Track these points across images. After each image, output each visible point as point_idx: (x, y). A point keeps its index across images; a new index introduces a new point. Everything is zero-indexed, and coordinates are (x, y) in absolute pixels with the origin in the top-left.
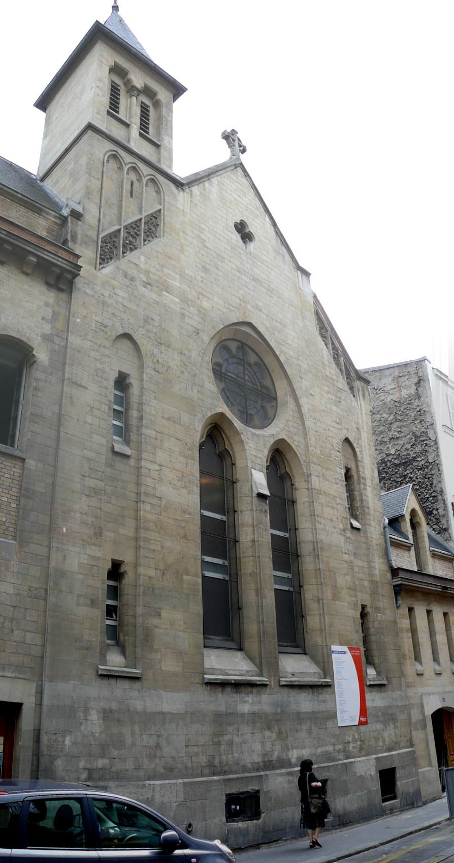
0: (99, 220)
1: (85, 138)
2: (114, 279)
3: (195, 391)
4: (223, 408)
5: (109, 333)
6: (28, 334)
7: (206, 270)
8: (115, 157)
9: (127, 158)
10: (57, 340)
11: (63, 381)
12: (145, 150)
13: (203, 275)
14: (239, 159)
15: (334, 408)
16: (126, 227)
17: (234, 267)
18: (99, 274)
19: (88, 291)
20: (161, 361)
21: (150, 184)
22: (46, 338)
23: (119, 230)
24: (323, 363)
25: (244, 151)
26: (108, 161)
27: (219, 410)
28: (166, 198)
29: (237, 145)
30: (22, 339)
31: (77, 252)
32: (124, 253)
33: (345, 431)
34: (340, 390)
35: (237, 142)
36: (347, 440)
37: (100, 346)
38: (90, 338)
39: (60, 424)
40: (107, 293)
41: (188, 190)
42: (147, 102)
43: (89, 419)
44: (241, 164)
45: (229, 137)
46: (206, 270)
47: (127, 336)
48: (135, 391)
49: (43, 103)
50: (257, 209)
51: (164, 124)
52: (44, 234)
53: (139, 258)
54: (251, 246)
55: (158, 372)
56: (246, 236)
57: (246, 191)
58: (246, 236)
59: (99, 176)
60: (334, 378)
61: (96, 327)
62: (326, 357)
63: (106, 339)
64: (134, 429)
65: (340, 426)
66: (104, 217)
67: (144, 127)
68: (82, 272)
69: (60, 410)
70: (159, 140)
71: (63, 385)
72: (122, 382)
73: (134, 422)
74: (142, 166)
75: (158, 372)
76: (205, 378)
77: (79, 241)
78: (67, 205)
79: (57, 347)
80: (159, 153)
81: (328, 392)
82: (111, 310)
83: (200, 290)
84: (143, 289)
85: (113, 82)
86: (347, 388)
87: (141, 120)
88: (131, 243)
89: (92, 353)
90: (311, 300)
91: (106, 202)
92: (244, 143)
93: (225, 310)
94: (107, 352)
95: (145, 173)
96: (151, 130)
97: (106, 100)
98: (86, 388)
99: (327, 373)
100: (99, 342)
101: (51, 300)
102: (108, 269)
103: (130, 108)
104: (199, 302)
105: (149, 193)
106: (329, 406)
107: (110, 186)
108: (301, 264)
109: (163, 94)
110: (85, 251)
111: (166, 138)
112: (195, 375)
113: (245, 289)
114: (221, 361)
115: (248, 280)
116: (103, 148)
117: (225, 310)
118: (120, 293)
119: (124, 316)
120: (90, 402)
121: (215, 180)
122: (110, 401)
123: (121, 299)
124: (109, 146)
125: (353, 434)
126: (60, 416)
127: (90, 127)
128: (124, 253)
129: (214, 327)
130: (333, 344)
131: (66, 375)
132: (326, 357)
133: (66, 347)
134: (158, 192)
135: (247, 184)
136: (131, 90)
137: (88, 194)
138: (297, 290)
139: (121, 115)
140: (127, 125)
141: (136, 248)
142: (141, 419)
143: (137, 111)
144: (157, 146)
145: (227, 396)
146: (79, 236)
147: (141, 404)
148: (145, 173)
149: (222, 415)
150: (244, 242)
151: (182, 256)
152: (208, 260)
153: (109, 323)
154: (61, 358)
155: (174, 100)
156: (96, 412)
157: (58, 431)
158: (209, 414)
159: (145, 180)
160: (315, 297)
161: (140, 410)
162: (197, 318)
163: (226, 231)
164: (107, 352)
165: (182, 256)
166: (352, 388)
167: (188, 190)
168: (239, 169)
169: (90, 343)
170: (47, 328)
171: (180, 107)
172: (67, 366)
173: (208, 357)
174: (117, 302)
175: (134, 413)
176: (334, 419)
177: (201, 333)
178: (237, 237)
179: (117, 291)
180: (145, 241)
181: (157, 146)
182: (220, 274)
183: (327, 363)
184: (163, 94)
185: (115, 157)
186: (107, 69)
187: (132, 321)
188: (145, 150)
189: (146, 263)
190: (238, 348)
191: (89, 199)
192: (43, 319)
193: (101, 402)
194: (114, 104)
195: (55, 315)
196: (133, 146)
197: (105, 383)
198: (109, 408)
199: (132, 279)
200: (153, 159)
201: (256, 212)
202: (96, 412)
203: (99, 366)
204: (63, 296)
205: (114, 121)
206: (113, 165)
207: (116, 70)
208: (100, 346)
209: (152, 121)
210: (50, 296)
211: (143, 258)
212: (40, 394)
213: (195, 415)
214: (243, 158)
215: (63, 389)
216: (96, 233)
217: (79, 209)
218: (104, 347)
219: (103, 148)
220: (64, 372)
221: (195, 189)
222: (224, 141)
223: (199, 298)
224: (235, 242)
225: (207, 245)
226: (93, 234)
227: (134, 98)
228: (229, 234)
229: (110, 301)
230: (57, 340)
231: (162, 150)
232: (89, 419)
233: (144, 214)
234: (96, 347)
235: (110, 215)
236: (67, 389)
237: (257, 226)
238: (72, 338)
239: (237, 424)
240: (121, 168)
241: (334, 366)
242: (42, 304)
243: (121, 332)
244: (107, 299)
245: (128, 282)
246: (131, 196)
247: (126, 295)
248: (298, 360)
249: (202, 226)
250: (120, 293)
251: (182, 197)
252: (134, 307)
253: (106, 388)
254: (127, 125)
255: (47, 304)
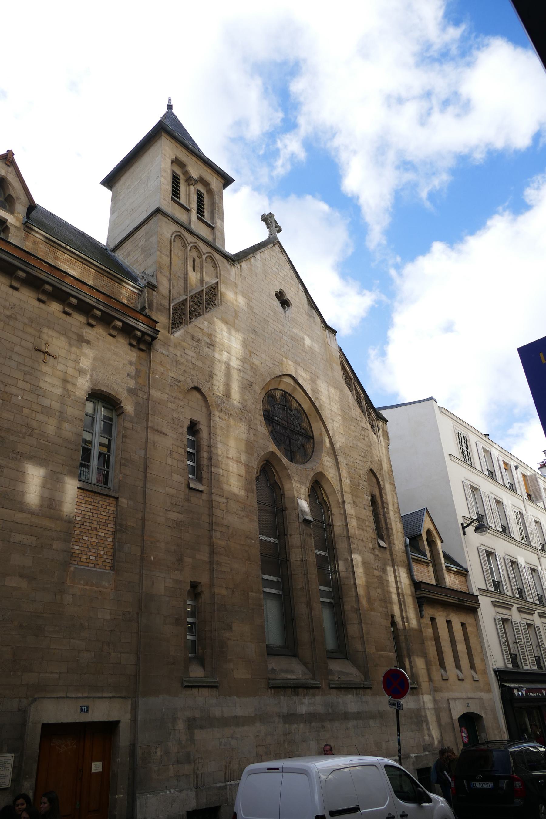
0: (170, 291)
1: (154, 220)
2: (184, 341)
3: (252, 434)
4: (272, 447)
5: (182, 387)
6: (116, 389)
7: (255, 332)
8: (180, 236)
9: (190, 239)
10: (140, 394)
11: (147, 428)
12: (203, 231)
13: (253, 336)
14: (276, 238)
15: (360, 444)
16: (191, 297)
17: (277, 329)
18: (172, 337)
19: (164, 352)
20: (224, 409)
21: (208, 260)
22: (132, 392)
23: (186, 299)
24: (349, 407)
25: (279, 231)
26: (174, 240)
27: (271, 450)
28: (222, 273)
29: (274, 226)
30: (112, 392)
31: (154, 318)
32: (190, 319)
33: (369, 463)
34: (364, 429)
35: (274, 223)
36: (371, 470)
37: (175, 398)
38: (167, 391)
39: (146, 467)
40: (179, 353)
41: (238, 265)
42: (202, 190)
43: (169, 461)
44: (278, 242)
45: (268, 219)
46: (255, 332)
47: (197, 389)
48: (204, 434)
49: (110, 182)
50: (292, 279)
51: (217, 210)
52: (125, 301)
53: (203, 323)
54: (289, 311)
55: (222, 419)
56: (285, 303)
57: (283, 264)
58: (285, 303)
59: (168, 253)
60: (359, 419)
61: (172, 382)
62: (351, 402)
63: (180, 392)
64: (205, 468)
65: (365, 460)
66: (173, 288)
67: (200, 211)
68: (159, 336)
69: (146, 454)
70: (213, 223)
71: (147, 432)
72: (193, 428)
73: (205, 462)
74: (201, 245)
75: (222, 419)
76: (258, 423)
77: (154, 309)
78: (143, 277)
79: (140, 400)
80: (214, 234)
81: (354, 431)
82: (183, 368)
83: (251, 349)
84: (207, 349)
85: (173, 172)
86: (369, 427)
87: (198, 205)
88: (196, 310)
89: (170, 404)
90: (337, 354)
91: (174, 275)
92: (279, 224)
93: (272, 366)
94: (181, 403)
95: (205, 251)
96: (206, 214)
97: (169, 187)
98: (166, 435)
99: (353, 415)
100: (174, 396)
101: (134, 360)
102: (179, 334)
103: (189, 196)
104: (251, 360)
105: (208, 267)
106: (355, 442)
107: (177, 262)
108: (329, 324)
109: (215, 182)
110: (159, 317)
111: (218, 222)
112: (251, 421)
113: (285, 346)
114: (269, 408)
115: (287, 339)
116: (167, 230)
117: (272, 366)
118: (190, 353)
119: (193, 372)
120: (169, 445)
121: (258, 256)
122: (184, 445)
123: (190, 358)
124: (174, 228)
125: (376, 465)
126: (146, 460)
127: (158, 211)
128: (190, 319)
129: (264, 380)
130: (356, 390)
131: (150, 424)
132: (351, 402)
133: (148, 400)
134: (215, 267)
135: (284, 258)
136: (189, 180)
137: (160, 268)
138: (326, 346)
139: (182, 201)
140: (188, 210)
141: (200, 315)
142: (210, 459)
143: (194, 197)
144: (212, 228)
145: (275, 436)
146: (155, 304)
147: (210, 446)
148: (205, 251)
149: (273, 453)
150: (284, 308)
151: (236, 321)
152: (256, 324)
153: (182, 378)
154: (145, 408)
155: (224, 189)
156: (175, 455)
157: (145, 472)
158: (263, 453)
159: (204, 258)
160: (341, 350)
161: (210, 452)
162: (249, 372)
163: (269, 299)
164: (181, 403)
165: (236, 321)
166: (373, 427)
167: (238, 265)
168: (277, 246)
169: (167, 396)
170: (132, 384)
171: (228, 195)
172: (150, 416)
173: (260, 406)
174: (187, 361)
175: (205, 455)
176: (360, 453)
177: (254, 385)
178: (277, 303)
179: (187, 351)
180: (206, 308)
181: (212, 228)
182: (266, 335)
183: (352, 407)
184: (215, 182)
185: (180, 236)
186: (170, 162)
187: (199, 376)
188: (203, 231)
189: (209, 327)
190: (281, 396)
191: (161, 272)
192: (128, 375)
193: (178, 446)
194: (176, 192)
195: (138, 371)
196: (193, 227)
197: (181, 430)
198: (185, 451)
199: (198, 341)
200: (210, 238)
201: (292, 282)
202: (175, 455)
203: (175, 415)
204: (143, 355)
205: (176, 206)
206: (177, 244)
207: (176, 162)
208: (175, 398)
209: (208, 207)
210: (133, 355)
211: (206, 323)
212: (128, 441)
213: (252, 455)
214: (279, 236)
215: (147, 436)
216: (168, 302)
217: (153, 281)
218: (179, 399)
219: (167, 230)
220: (147, 420)
221: (244, 265)
222: (264, 223)
223: (251, 356)
224: (276, 308)
225: (255, 311)
226: (165, 302)
227: (192, 187)
228: (272, 301)
229: (182, 360)
230: (140, 394)
231: (216, 231)
232: (169, 461)
233: (205, 287)
234: (172, 399)
235: (178, 285)
236: (151, 436)
237: (293, 294)
238: (152, 392)
239: (285, 461)
240: (185, 246)
241: (358, 408)
242: (126, 362)
243: (192, 386)
244: (179, 358)
245: (195, 344)
246: (194, 271)
247: (194, 355)
248: (330, 404)
249: (251, 295)
250: (190, 353)
251: (233, 273)
252: (200, 365)
253: (182, 434)
254: (188, 210)
255: (131, 363)
